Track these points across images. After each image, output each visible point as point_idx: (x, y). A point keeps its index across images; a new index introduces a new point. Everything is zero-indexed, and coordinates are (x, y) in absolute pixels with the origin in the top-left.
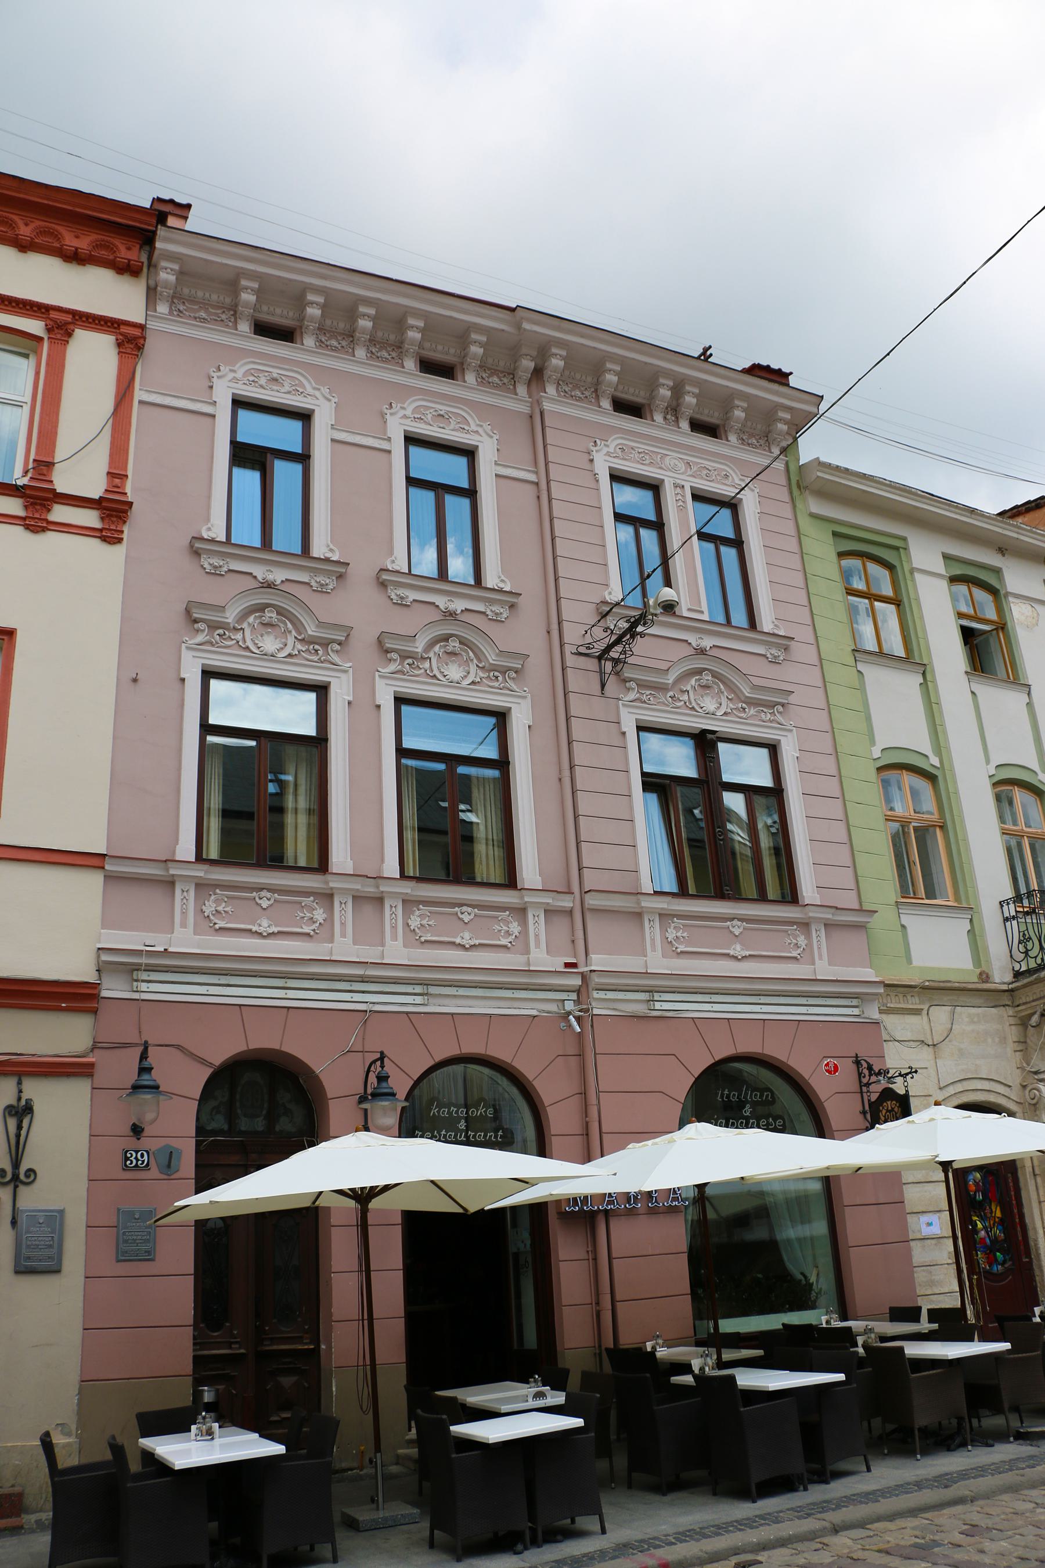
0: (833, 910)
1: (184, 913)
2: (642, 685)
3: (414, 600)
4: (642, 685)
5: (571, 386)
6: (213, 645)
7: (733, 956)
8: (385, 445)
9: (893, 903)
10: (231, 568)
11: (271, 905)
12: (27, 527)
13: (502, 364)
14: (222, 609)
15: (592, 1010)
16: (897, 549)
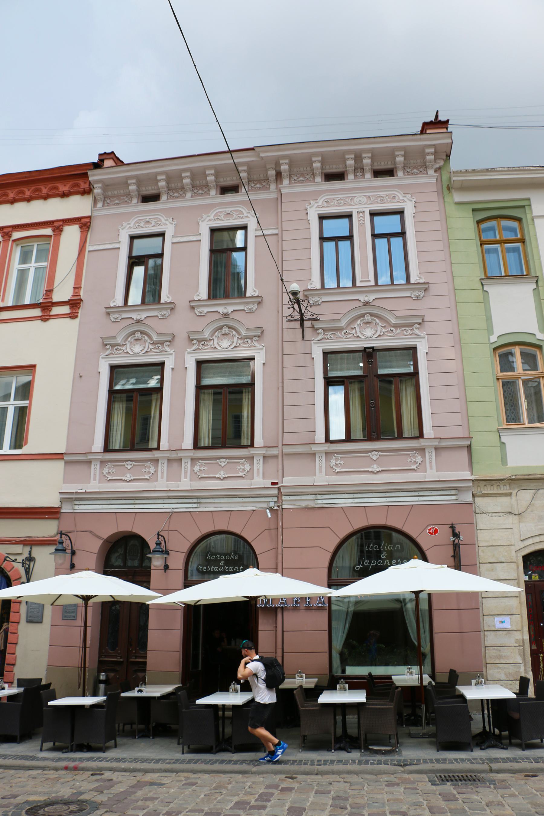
0: (438, 440)
1: (95, 475)
2: (325, 330)
3: (208, 312)
4: (325, 330)
5: (298, 175)
6: (113, 354)
7: (371, 472)
8: (198, 238)
9: (496, 429)
10: (123, 317)
11: (132, 467)
12: (42, 320)
13: (262, 176)
14: (115, 337)
15: (282, 506)
16: (523, 207)
